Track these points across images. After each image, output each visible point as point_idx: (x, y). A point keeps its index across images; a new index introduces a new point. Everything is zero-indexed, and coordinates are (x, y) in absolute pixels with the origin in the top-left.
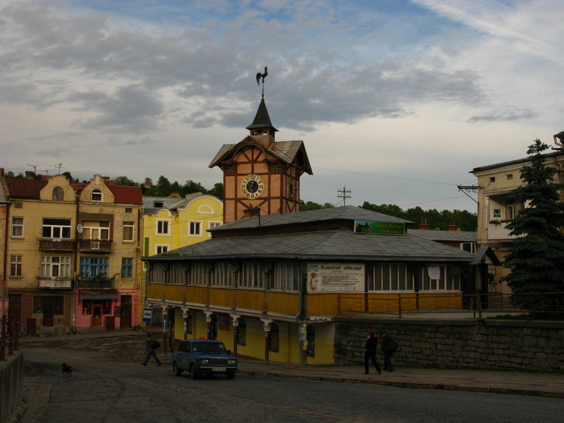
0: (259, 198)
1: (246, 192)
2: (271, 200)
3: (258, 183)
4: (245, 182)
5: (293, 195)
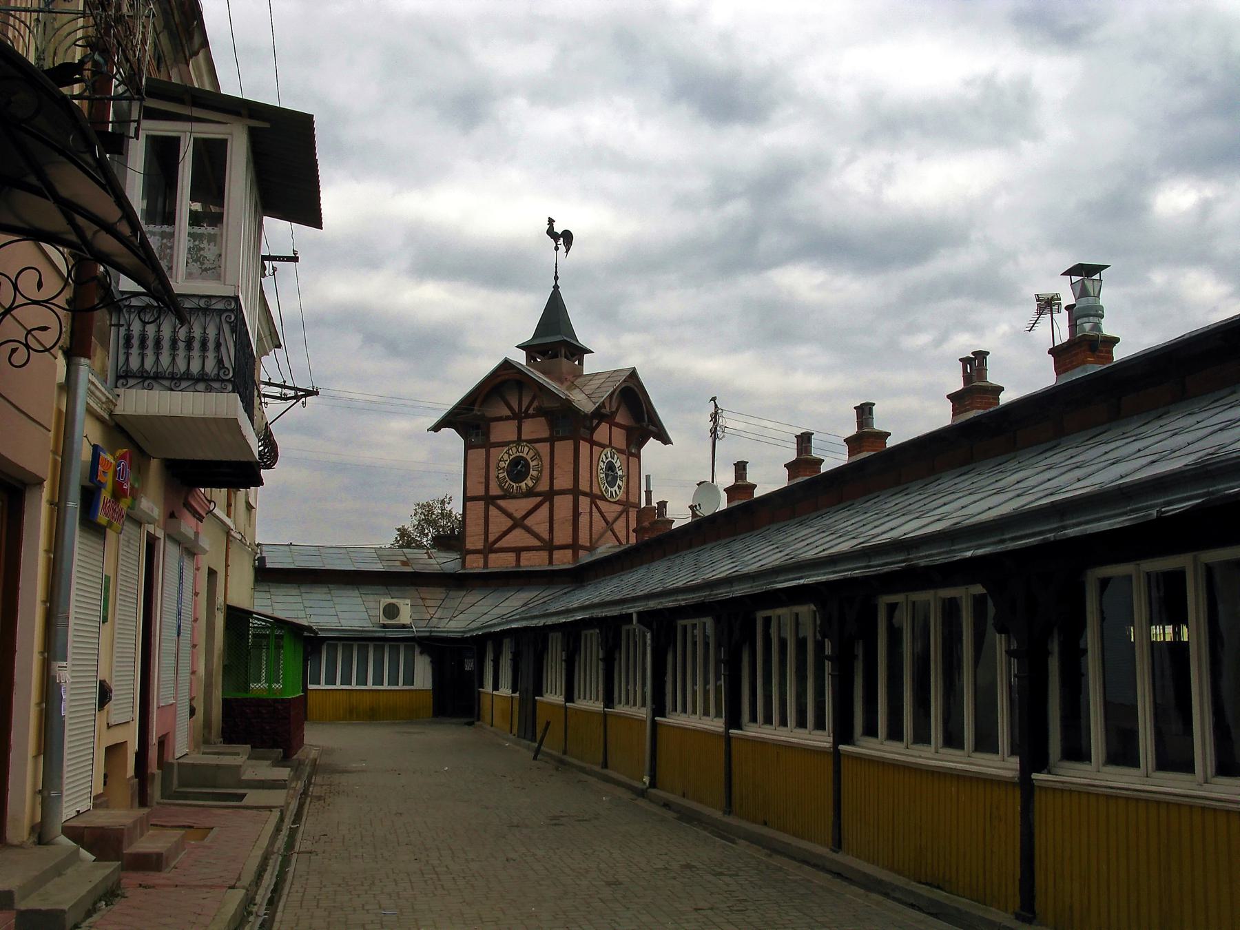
0: (530, 493)
1: (507, 481)
2: (557, 499)
3: (530, 461)
5: (616, 488)
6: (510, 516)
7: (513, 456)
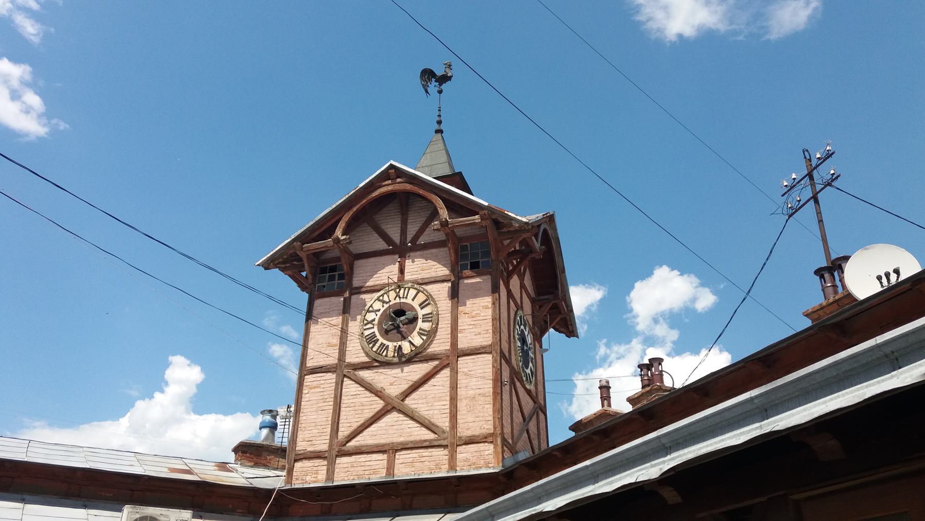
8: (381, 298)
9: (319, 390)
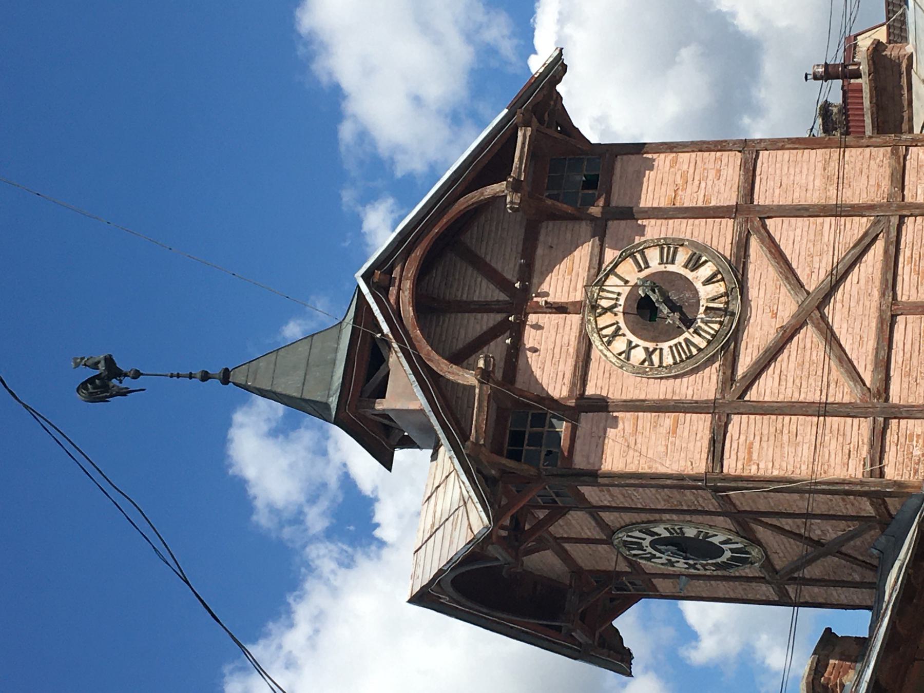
1: (686, 340)
4: (630, 346)
6: (787, 336)
7: (622, 324)
8: (605, 340)
9: (756, 445)
